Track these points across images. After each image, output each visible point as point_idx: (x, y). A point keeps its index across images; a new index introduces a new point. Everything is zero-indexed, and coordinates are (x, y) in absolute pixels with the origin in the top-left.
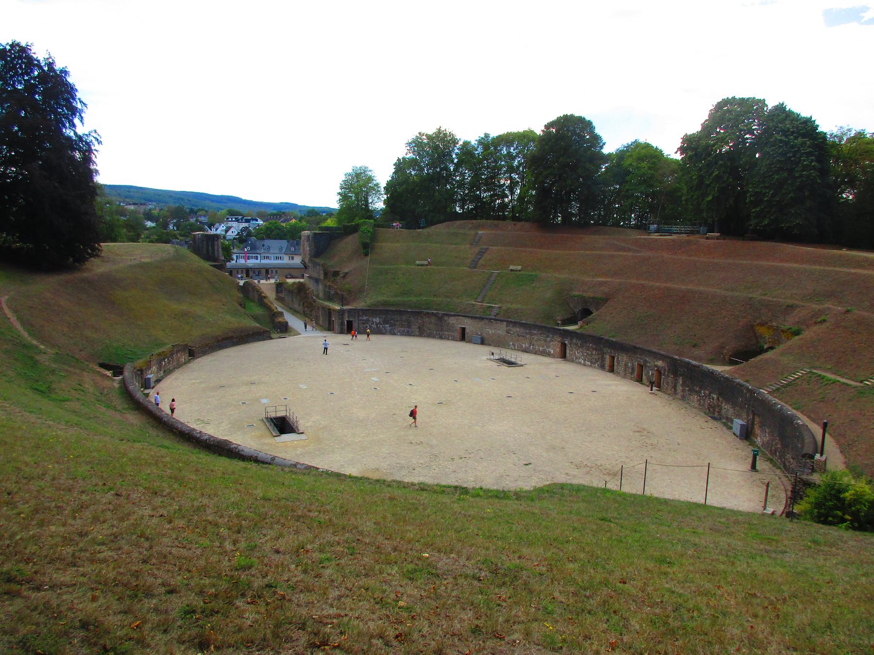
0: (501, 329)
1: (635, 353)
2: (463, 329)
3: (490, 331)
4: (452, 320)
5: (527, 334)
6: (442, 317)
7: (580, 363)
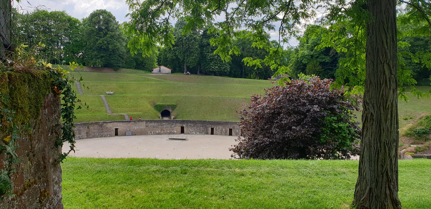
0: (142, 126)
1: (227, 124)
2: (116, 130)
3: (135, 127)
4: (109, 125)
5: (159, 125)
6: (102, 125)
7: (193, 134)
